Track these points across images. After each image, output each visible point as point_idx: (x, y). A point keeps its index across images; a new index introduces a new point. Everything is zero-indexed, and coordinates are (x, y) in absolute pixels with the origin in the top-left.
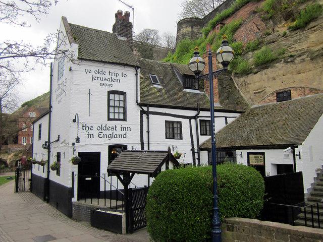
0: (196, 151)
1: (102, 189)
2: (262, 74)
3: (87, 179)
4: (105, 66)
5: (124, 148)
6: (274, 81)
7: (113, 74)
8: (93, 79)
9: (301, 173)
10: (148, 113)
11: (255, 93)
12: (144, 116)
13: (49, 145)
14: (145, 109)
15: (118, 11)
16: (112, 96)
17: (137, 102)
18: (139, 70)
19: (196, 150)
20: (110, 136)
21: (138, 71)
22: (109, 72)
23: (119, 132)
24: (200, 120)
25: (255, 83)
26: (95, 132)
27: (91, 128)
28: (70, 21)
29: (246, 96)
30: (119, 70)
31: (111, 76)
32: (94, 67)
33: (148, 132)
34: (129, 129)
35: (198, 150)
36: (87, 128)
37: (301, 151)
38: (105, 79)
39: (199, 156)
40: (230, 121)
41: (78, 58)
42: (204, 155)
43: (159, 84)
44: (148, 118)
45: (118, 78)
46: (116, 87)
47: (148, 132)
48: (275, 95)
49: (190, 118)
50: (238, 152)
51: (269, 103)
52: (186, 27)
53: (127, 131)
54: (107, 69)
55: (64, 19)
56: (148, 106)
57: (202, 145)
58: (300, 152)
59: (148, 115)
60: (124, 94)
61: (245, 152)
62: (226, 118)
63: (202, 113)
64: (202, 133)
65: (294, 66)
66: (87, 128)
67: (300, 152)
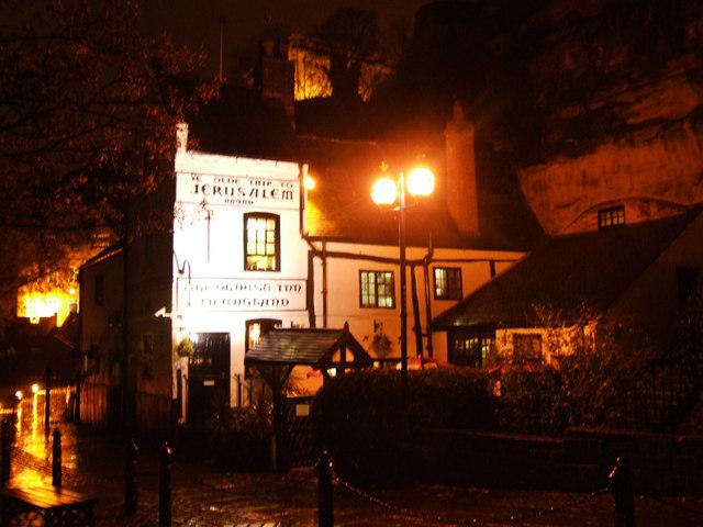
0: (424, 331)
1: (233, 404)
3: (206, 383)
12: (317, 261)
14: (319, 245)
33: (325, 292)
35: (427, 329)
39: (430, 342)
40: (500, 268)
44: (324, 264)
60: (276, 218)
62: (492, 263)
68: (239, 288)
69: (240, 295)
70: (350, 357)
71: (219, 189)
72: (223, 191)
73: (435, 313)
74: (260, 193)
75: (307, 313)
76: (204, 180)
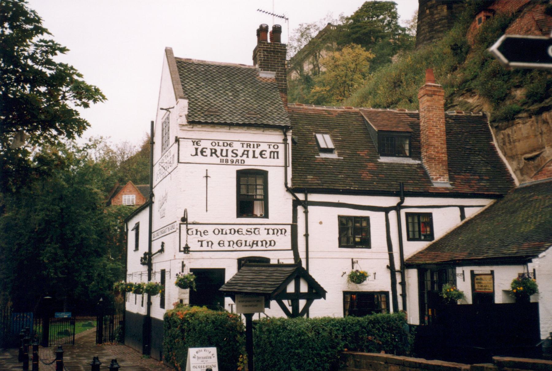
4: (232, 130)
5: (265, 261)
10: (306, 204)
12: (300, 209)
13: (150, 260)
14: (301, 197)
19: (397, 266)
21: (288, 134)
24: (408, 215)
28: (177, 54)
33: (307, 235)
37: (536, 267)
40: (470, 213)
42: (412, 275)
44: (306, 212)
47: (307, 235)
49: (386, 210)
50: (459, 270)
55: (168, 52)
56: (307, 191)
57: (410, 259)
58: (534, 270)
59: (306, 208)
61: (467, 270)
62: (462, 208)
63: (409, 201)
64: (411, 236)
67: (534, 270)
68: (233, 231)
69: (236, 237)
70: (304, 288)
71: (216, 151)
72: (218, 153)
73: (408, 254)
74: (251, 154)
75: (291, 252)
76: (203, 144)
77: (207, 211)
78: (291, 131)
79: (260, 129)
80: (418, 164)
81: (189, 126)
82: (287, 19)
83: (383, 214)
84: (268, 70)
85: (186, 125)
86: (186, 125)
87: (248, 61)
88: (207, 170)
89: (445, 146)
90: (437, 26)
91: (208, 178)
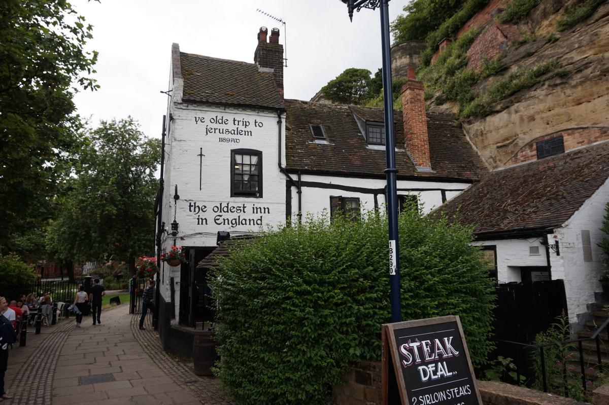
2: (509, 113)
4: (227, 110)
6: (532, 123)
7: (241, 123)
8: (208, 131)
9: (560, 283)
10: (299, 185)
11: (498, 147)
12: (294, 190)
14: (294, 177)
15: (261, 30)
16: (239, 158)
17: (280, 164)
18: (284, 116)
20: (234, 222)
21: (282, 116)
22: (234, 120)
23: (249, 215)
25: (499, 129)
26: (210, 215)
27: (203, 209)
28: (182, 50)
29: (485, 154)
30: (250, 117)
31: (237, 126)
32: (209, 114)
34: (267, 210)
36: (197, 209)
38: (227, 131)
40: (450, 196)
41: (183, 100)
43: (324, 139)
44: (299, 193)
45: (248, 129)
46: (245, 143)
48: (535, 147)
49: (375, 192)
51: (524, 163)
52: (400, 58)
53: (263, 214)
54: (230, 116)
55: (175, 47)
56: (300, 172)
58: (557, 242)
60: (259, 154)
65: (568, 91)
66: (197, 209)
67: (557, 242)
77: (201, 189)
78: (285, 114)
79: (254, 110)
80: (403, 152)
81: (184, 105)
82: (284, 23)
83: (373, 195)
84: (267, 67)
85: (180, 104)
86: (180, 104)
87: (250, 59)
88: (201, 148)
89: (427, 135)
90: (401, 71)
91: (203, 156)
